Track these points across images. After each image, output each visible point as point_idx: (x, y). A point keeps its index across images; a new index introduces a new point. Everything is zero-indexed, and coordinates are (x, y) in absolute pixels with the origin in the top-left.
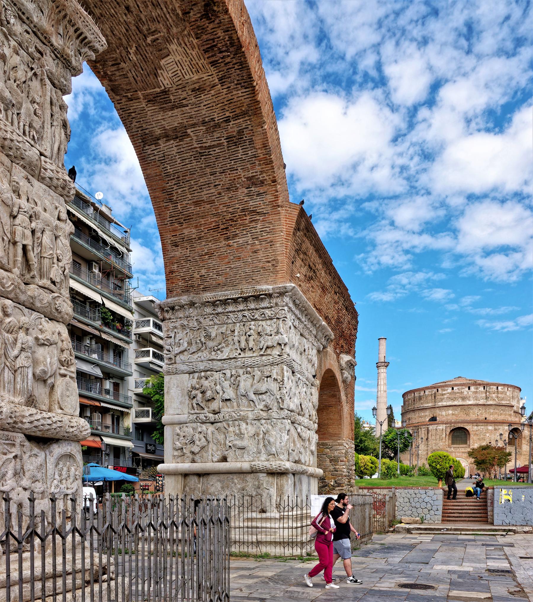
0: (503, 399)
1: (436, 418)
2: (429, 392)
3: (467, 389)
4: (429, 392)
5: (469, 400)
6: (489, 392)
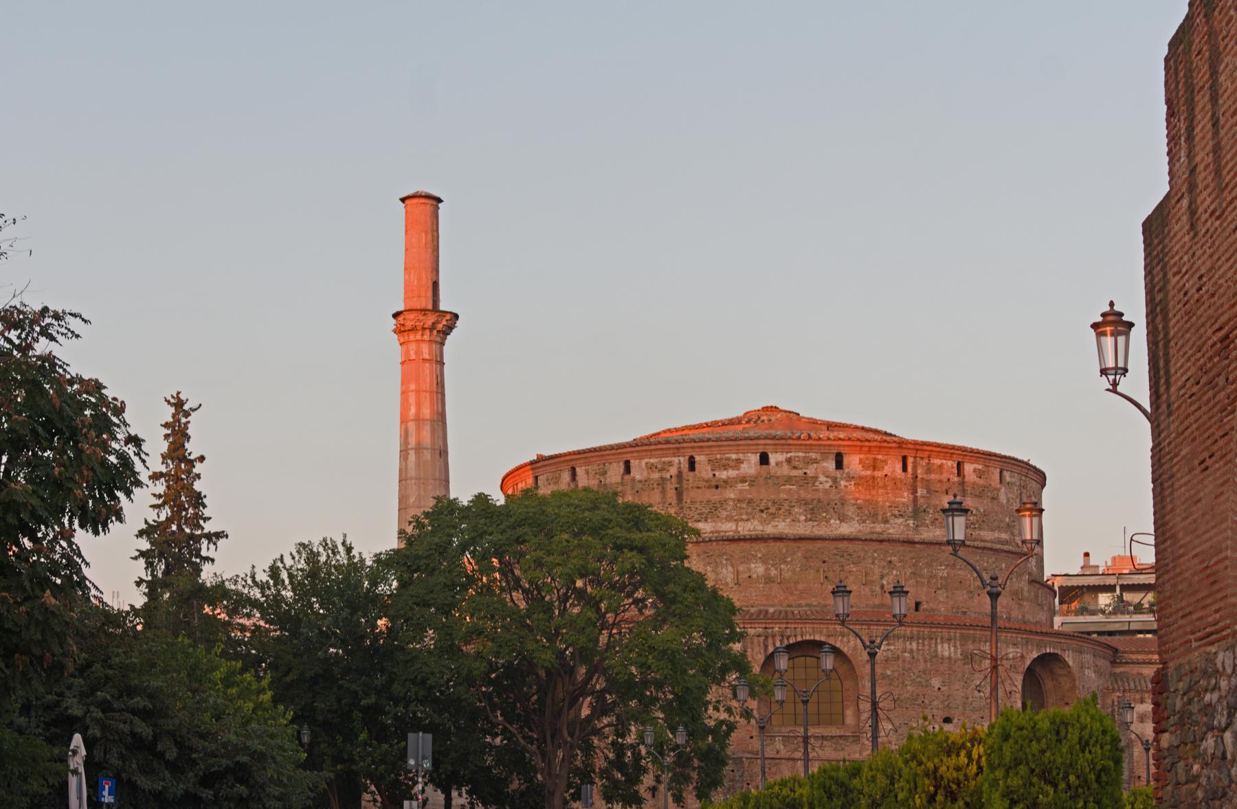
3: (830, 465)
5: (843, 519)
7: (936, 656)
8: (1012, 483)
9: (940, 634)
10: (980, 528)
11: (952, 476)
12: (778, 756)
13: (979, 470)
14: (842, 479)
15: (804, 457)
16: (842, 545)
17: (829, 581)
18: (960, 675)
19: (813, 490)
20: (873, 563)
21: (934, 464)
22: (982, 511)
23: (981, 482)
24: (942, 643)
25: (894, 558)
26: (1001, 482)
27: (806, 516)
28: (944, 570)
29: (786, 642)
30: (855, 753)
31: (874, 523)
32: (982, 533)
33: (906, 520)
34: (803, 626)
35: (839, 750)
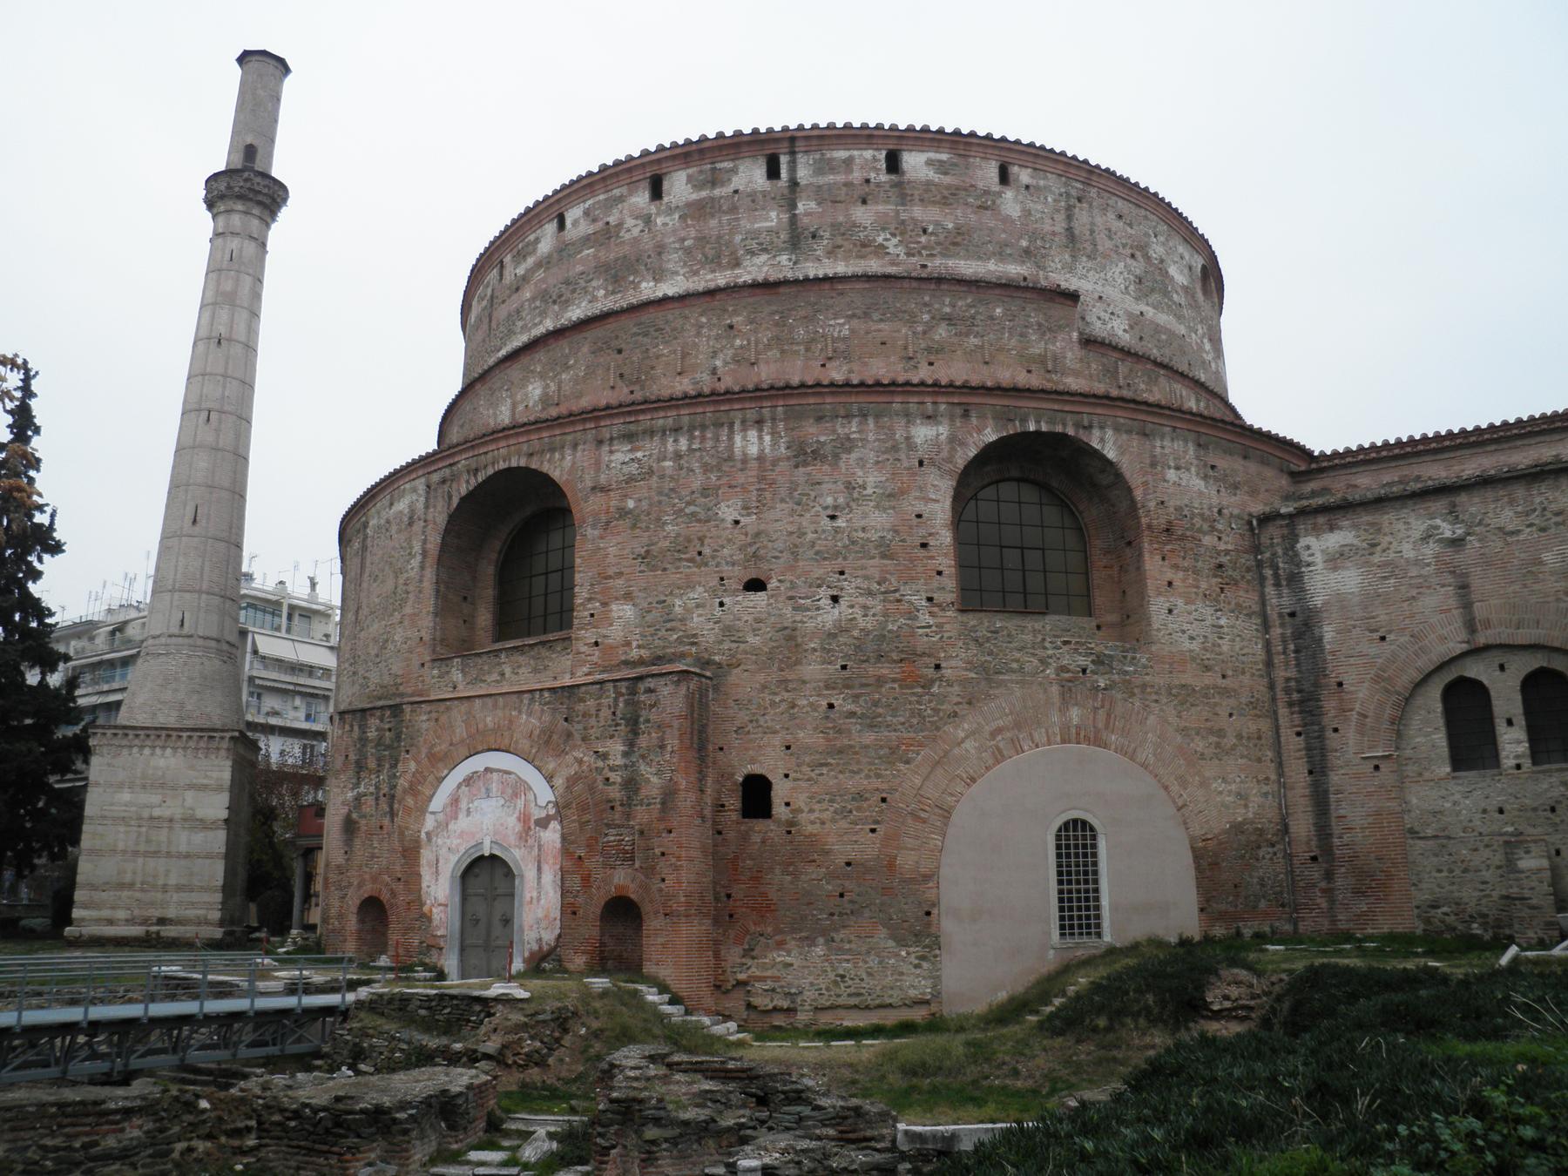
0: (957, 241)
3: (641, 198)
5: (659, 276)
6: (820, 194)
7: (731, 458)
8: (1038, 188)
9: (739, 415)
10: (944, 255)
11: (873, 175)
13: (940, 161)
14: (658, 214)
15: (606, 200)
16: (647, 316)
18: (783, 492)
20: (698, 334)
21: (833, 159)
22: (950, 226)
23: (947, 180)
24: (744, 430)
26: (1004, 177)
27: (606, 289)
28: (843, 324)
29: (473, 483)
31: (713, 271)
32: (950, 263)
34: (494, 447)
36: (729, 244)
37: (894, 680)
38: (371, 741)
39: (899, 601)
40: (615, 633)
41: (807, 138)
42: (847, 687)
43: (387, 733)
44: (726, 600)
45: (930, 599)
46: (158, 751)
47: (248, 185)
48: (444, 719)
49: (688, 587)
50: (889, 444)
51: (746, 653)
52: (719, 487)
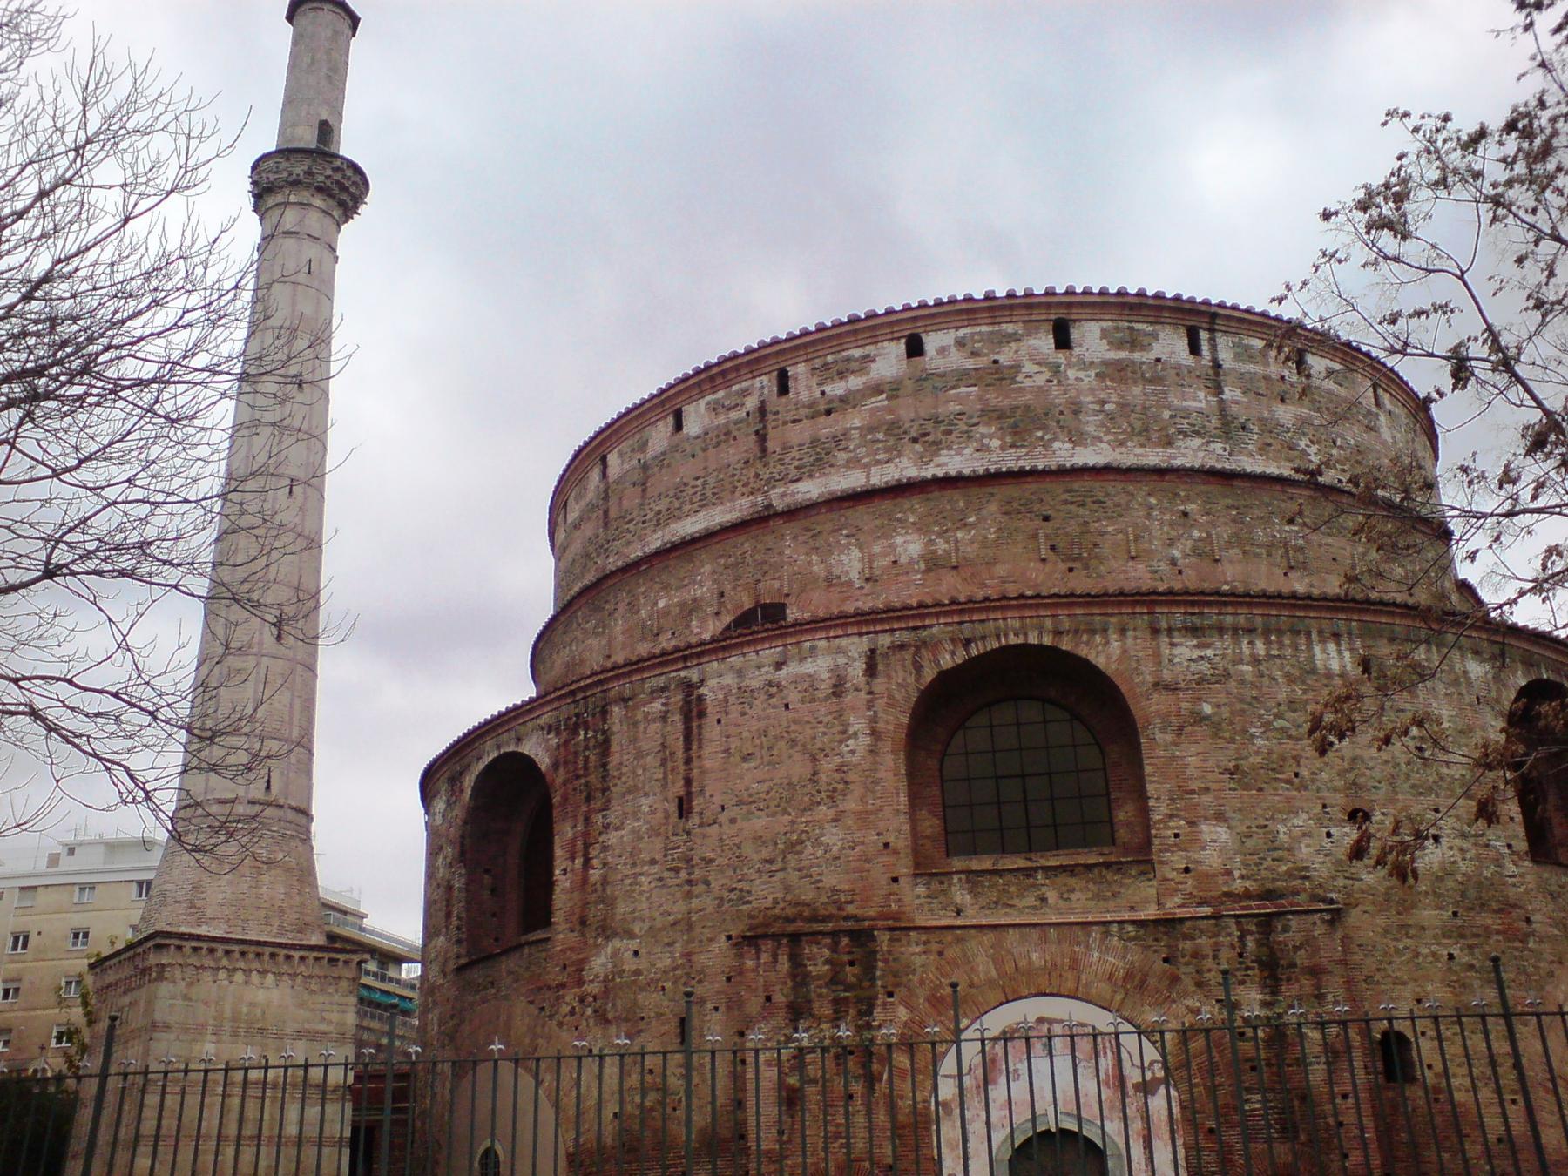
1: (783, 607)
2: (715, 408)
3: (1045, 342)
4: (715, 408)
7: (1313, 671)
9: (1314, 623)
11: (1286, 373)
12: (959, 922)
14: (1069, 366)
17: (1057, 554)
19: (1014, 389)
20: (1149, 516)
22: (1352, 442)
23: (1342, 392)
25: (1190, 507)
27: (1002, 439)
30: (1146, 901)
31: (1142, 446)
33: (1208, 442)
35: (1105, 899)
36: (1157, 418)
37: (1498, 932)
38: (819, 977)
39: (1487, 846)
40: (1211, 859)
41: (1228, 318)
42: (1462, 936)
43: (848, 968)
44: (1333, 831)
45: (1509, 846)
46: (255, 977)
47: (338, 177)
48: (951, 953)
49: (1290, 812)
50: (1452, 677)
51: (1363, 892)
52: (1307, 702)
